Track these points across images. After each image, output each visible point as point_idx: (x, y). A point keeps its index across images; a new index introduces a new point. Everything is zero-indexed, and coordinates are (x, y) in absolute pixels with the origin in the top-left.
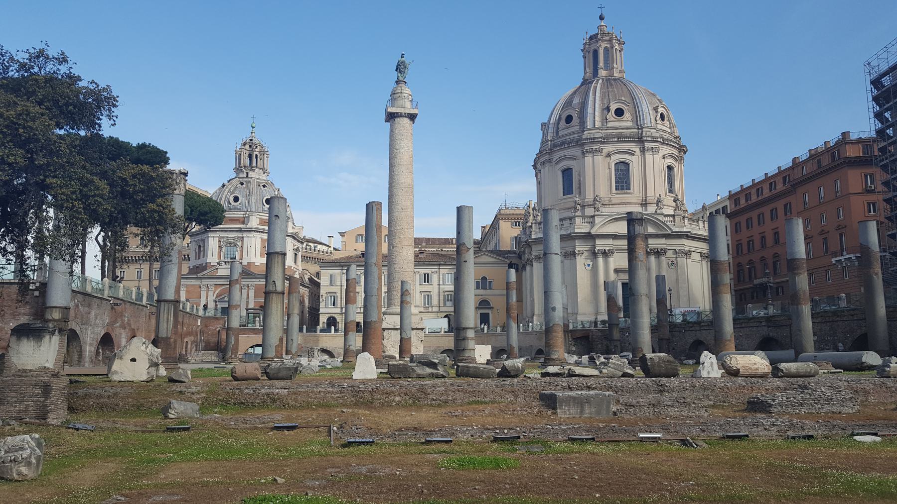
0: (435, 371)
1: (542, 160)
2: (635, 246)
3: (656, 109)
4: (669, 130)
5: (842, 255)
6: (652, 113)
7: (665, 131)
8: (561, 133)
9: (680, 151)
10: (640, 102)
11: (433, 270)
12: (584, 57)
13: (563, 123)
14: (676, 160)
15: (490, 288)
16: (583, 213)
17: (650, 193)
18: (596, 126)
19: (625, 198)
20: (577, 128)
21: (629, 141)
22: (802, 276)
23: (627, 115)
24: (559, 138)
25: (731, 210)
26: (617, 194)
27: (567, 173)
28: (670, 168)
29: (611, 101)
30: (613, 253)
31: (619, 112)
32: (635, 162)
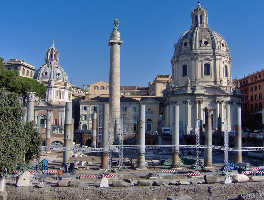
0: (129, 184)
1: (175, 60)
4: (225, 51)
6: (219, 43)
11: (128, 105)
12: (192, 18)
13: (183, 46)
15: (152, 114)
17: (218, 77)
27: (185, 67)
31: (206, 43)
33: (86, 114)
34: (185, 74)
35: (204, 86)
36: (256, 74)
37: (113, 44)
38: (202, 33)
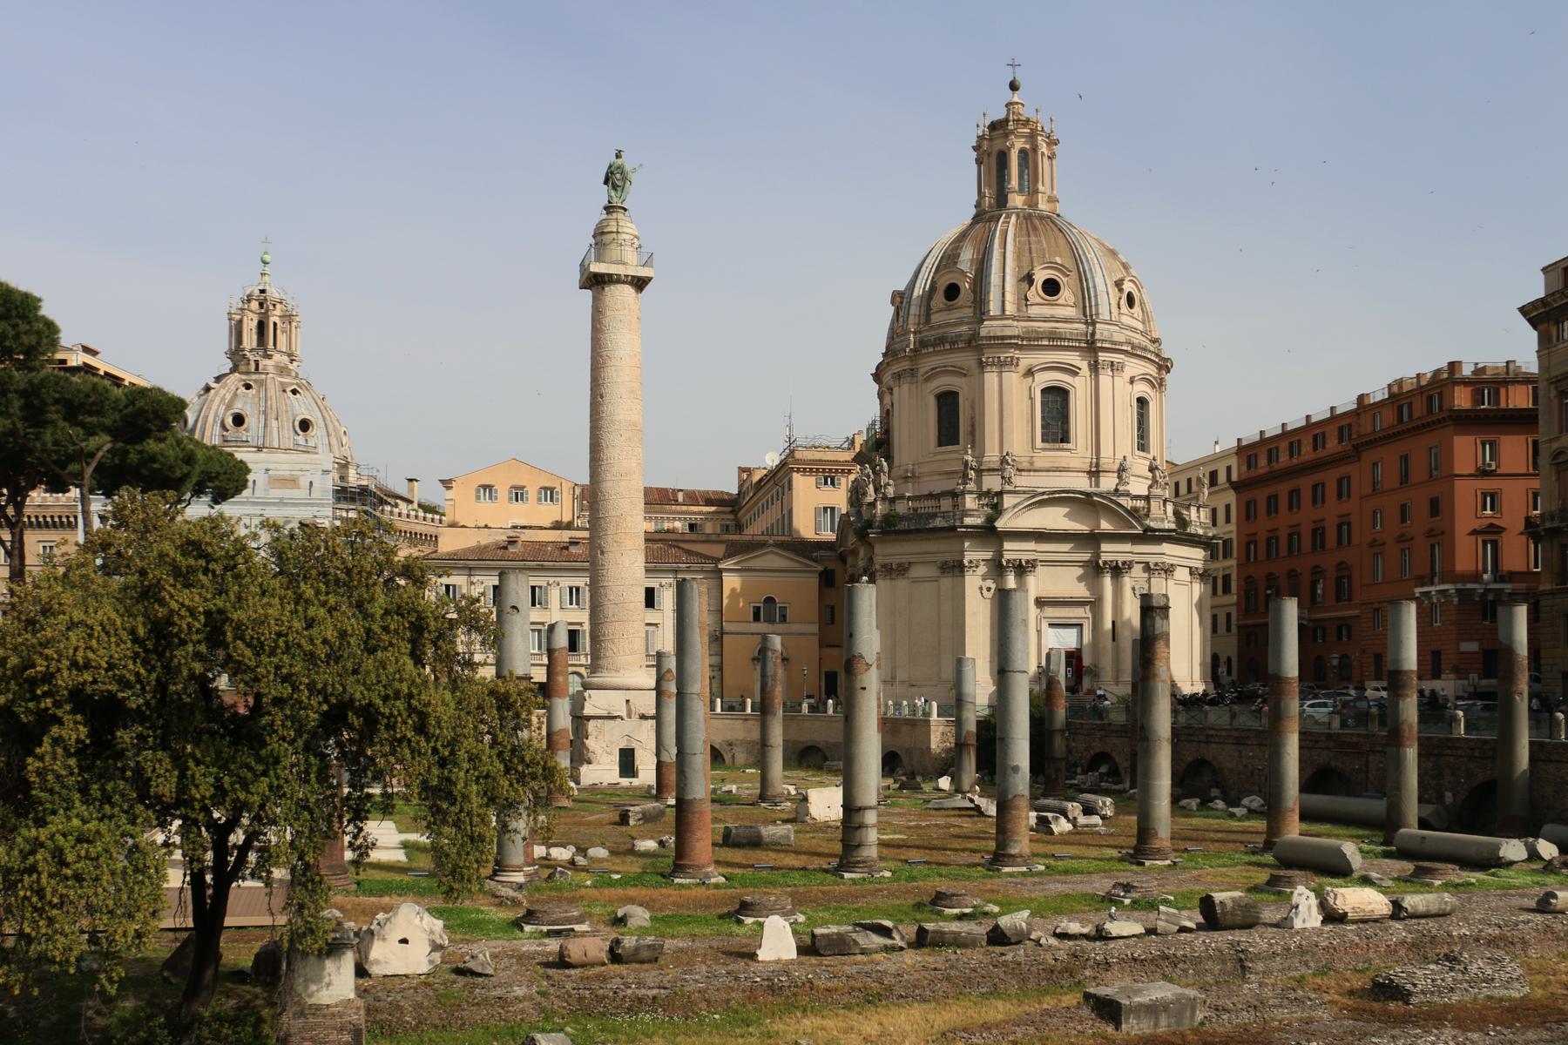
0: (889, 942)
1: (896, 368)
2: (1153, 655)
3: (1119, 284)
4: (1140, 327)
5: (1432, 584)
6: (1113, 291)
7: (1134, 330)
8: (935, 319)
9: (1160, 368)
10: (1091, 270)
12: (979, 162)
13: (939, 300)
14: (1153, 386)
16: (979, 482)
17: (1106, 452)
18: (1007, 313)
19: (1060, 459)
20: (969, 312)
21: (1068, 346)
22: (1409, 700)
23: (1066, 295)
24: (932, 328)
25: (1239, 475)
26: (1044, 449)
27: (948, 403)
28: (1142, 402)
29: (1035, 264)
30: (1034, 567)
31: (1051, 287)
32: (1079, 389)
33: (580, 624)
34: (948, 431)
35: (1043, 493)
36: (1277, 436)
37: (604, 283)
38: (1033, 239)
